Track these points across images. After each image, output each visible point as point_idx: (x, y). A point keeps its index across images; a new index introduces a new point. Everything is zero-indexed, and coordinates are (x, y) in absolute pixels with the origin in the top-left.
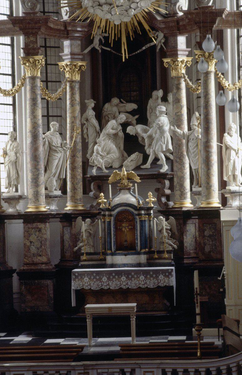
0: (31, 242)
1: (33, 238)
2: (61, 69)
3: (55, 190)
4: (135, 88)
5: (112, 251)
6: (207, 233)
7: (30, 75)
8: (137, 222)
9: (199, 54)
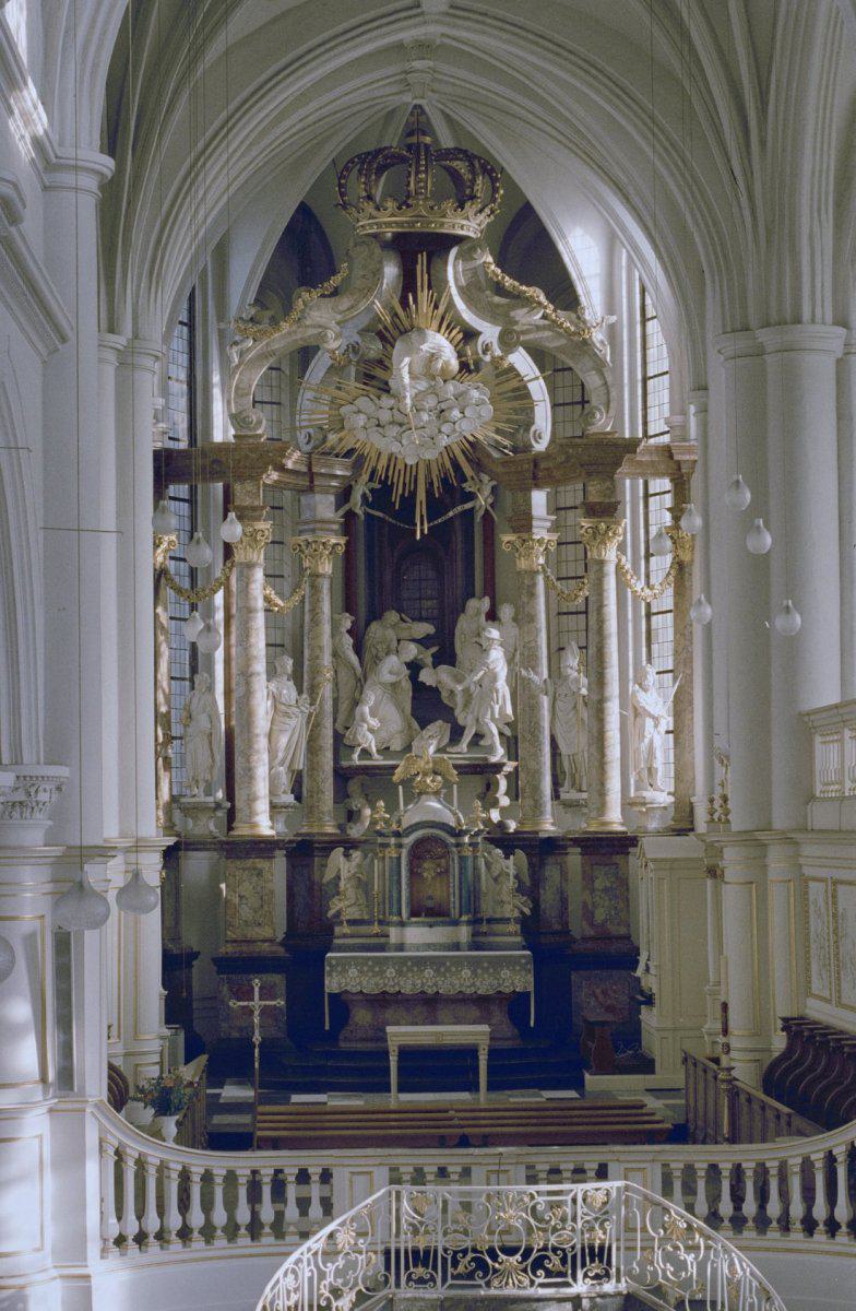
0: (241, 897)
1: (246, 888)
2: (294, 550)
3: (284, 792)
4: (429, 592)
6: (598, 884)
7: (243, 560)
8: (453, 860)
9: (587, 525)
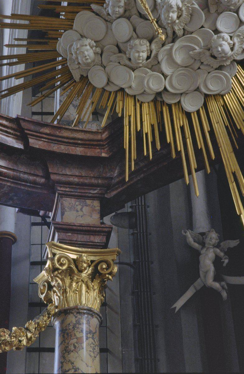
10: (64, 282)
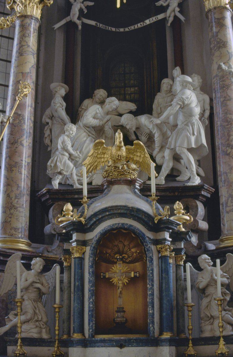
4: (132, 82)
5: (83, 334)
8: (152, 260)
10: (26, 1)
